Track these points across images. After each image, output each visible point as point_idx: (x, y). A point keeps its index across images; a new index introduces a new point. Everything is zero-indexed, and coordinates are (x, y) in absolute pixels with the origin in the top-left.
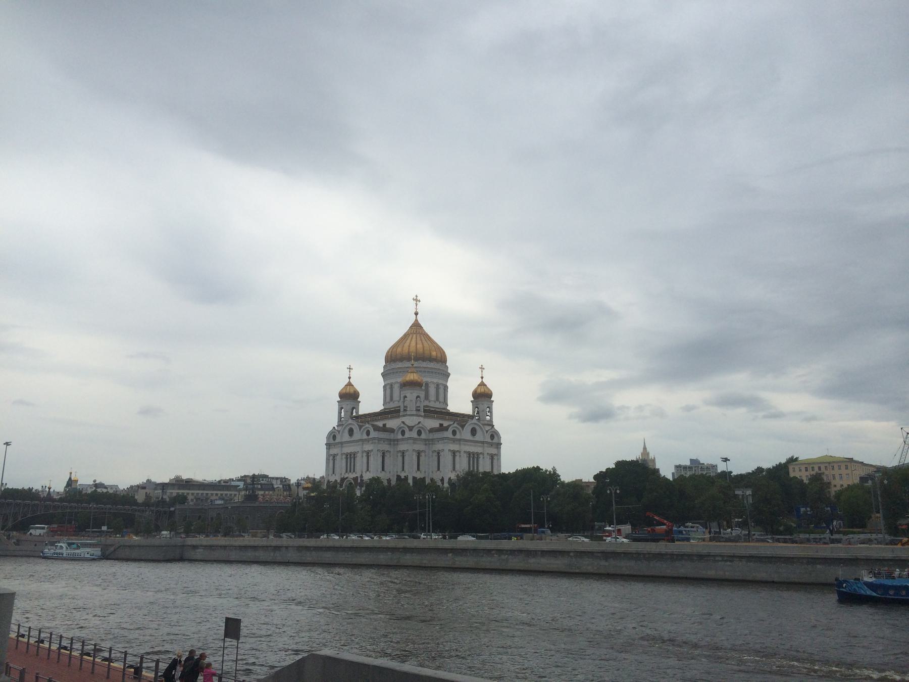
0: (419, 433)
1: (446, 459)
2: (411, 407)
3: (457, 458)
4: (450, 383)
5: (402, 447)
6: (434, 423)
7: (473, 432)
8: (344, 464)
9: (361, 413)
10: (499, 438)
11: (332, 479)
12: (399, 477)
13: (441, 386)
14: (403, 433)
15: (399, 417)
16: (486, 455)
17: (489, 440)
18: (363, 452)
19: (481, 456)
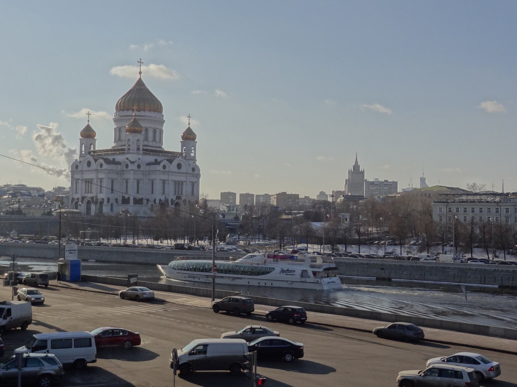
0: (139, 166)
1: (158, 186)
2: (134, 147)
3: (166, 185)
4: (165, 128)
5: (126, 176)
6: (151, 158)
7: (179, 166)
8: (84, 187)
9: (97, 149)
10: (199, 170)
11: (76, 196)
12: (123, 198)
13: (158, 131)
14: (127, 166)
15: (124, 153)
16: (188, 182)
17: (191, 172)
18: (97, 178)
19: (185, 183)
